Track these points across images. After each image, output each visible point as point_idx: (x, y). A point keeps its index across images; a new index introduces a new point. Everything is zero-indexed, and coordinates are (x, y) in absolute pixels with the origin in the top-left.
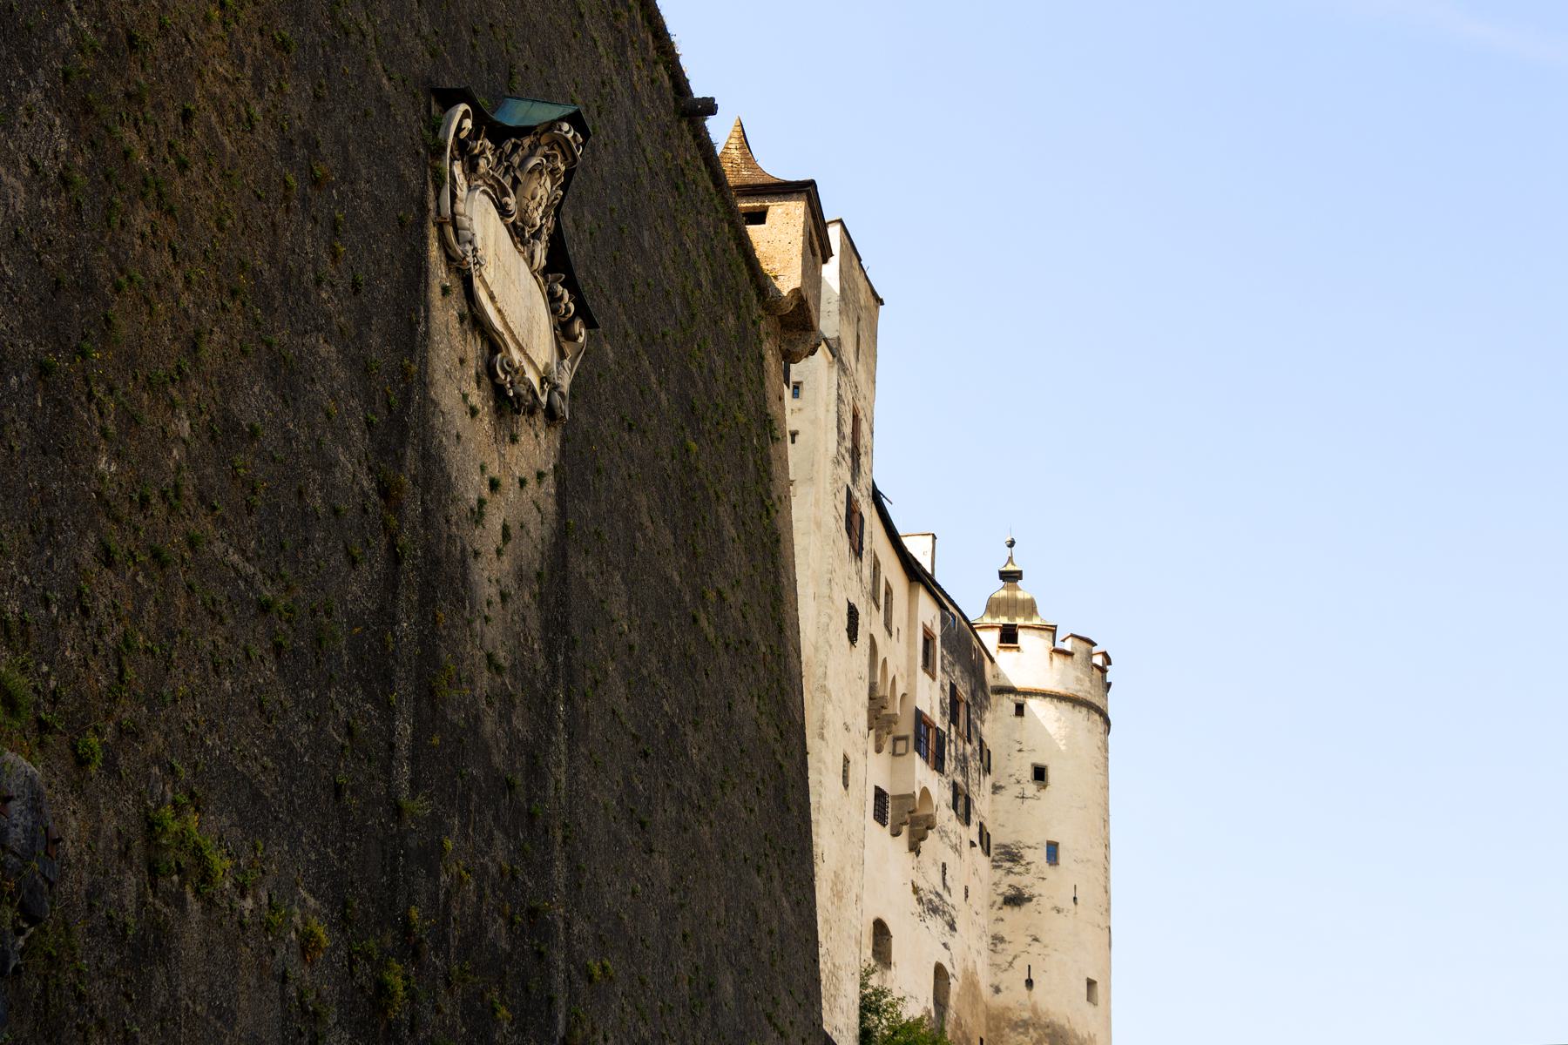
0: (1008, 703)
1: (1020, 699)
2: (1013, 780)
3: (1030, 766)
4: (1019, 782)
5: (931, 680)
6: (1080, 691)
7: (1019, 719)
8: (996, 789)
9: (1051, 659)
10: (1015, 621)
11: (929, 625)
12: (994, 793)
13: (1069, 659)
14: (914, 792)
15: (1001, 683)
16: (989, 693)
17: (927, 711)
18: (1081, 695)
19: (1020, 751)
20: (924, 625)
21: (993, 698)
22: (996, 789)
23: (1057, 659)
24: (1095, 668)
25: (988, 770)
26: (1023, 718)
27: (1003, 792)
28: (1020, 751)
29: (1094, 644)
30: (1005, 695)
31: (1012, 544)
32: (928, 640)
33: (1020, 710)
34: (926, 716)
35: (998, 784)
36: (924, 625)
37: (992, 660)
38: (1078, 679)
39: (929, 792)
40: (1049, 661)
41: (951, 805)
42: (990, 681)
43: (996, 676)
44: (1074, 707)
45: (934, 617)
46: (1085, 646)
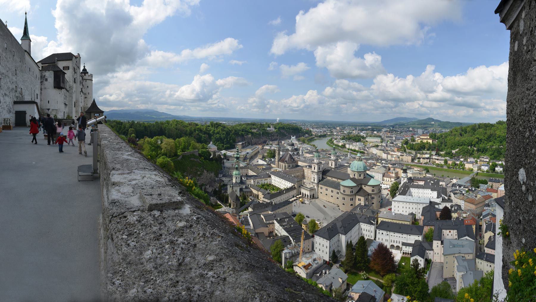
0: (85, 80)
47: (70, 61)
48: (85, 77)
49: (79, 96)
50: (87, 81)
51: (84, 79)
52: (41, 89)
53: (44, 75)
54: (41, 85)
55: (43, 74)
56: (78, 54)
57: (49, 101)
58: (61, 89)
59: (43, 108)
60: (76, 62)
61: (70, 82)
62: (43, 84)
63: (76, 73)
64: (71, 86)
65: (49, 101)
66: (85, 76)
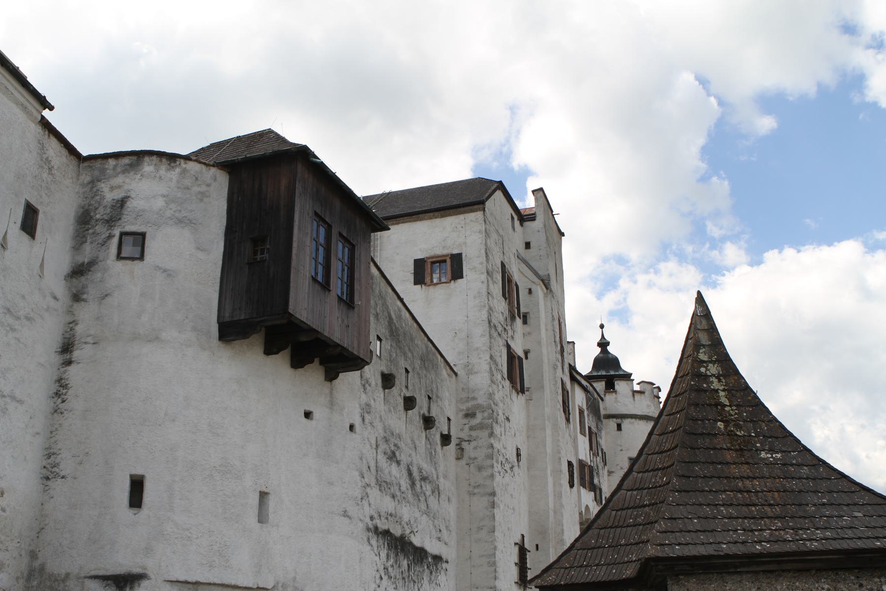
0: (612, 424)
1: (619, 421)
2: (619, 467)
3: (627, 458)
4: (622, 468)
5: (584, 437)
6: (650, 412)
7: (619, 432)
8: (610, 473)
9: (634, 396)
10: (609, 372)
11: (581, 405)
12: (609, 475)
13: (643, 395)
14: (582, 511)
15: (609, 412)
16: (602, 419)
17: (584, 459)
18: (650, 414)
19: (621, 450)
20: (579, 406)
21: (605, 421)
22: (610, 473)
23: (637, 396)
24: (655, 398)
25: (605, 464)
26: (622, 432)
27: (614, 474)
28: (621, 450)
29: (653, 384)
30: (611, 419)
31: (602, 326)
32: (581, 412)
33: (619, 427)
34: (584, 461)
35: (610, 470)
36: (579, 406)
37: (602, 400)
38: (648, 406)
39: (588, 507)
40: (632, 398)
41: (594, 499)
42: (603, 412)
43: (605, 409)
44: (647, 422)
45: (583, 399)
46: (649, 386)
47: (472, 216)
48: (611, 403)
49: (558, 496)
50: (626, 424)
51: (609, 416)
52: (67, 348)
53: (110, 196)
54: (77, 297)
55: (104, 187)
56: (539, 192)
57: (137, 486)
58: (331, 376)
59: (56, 566)
60: (528, 245)
61: (470, 370)
62: (92, 293)
63: (525, 320)
64: (482, 400)
65: (137, 486)
66: (609, 398)
